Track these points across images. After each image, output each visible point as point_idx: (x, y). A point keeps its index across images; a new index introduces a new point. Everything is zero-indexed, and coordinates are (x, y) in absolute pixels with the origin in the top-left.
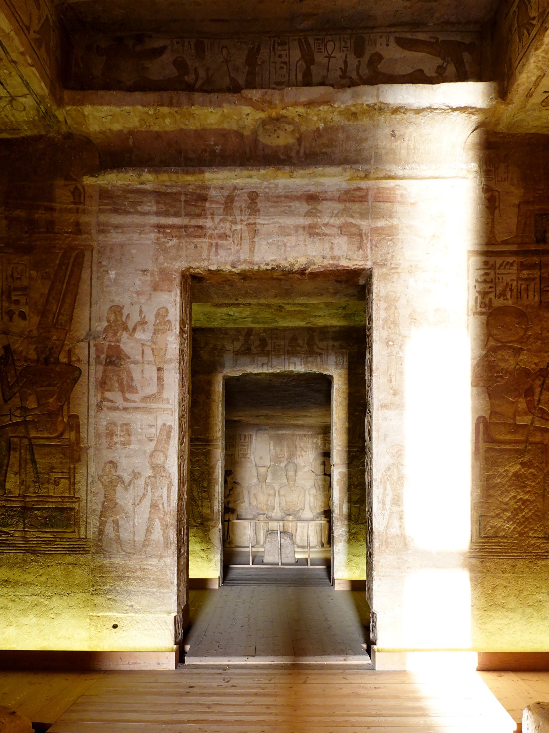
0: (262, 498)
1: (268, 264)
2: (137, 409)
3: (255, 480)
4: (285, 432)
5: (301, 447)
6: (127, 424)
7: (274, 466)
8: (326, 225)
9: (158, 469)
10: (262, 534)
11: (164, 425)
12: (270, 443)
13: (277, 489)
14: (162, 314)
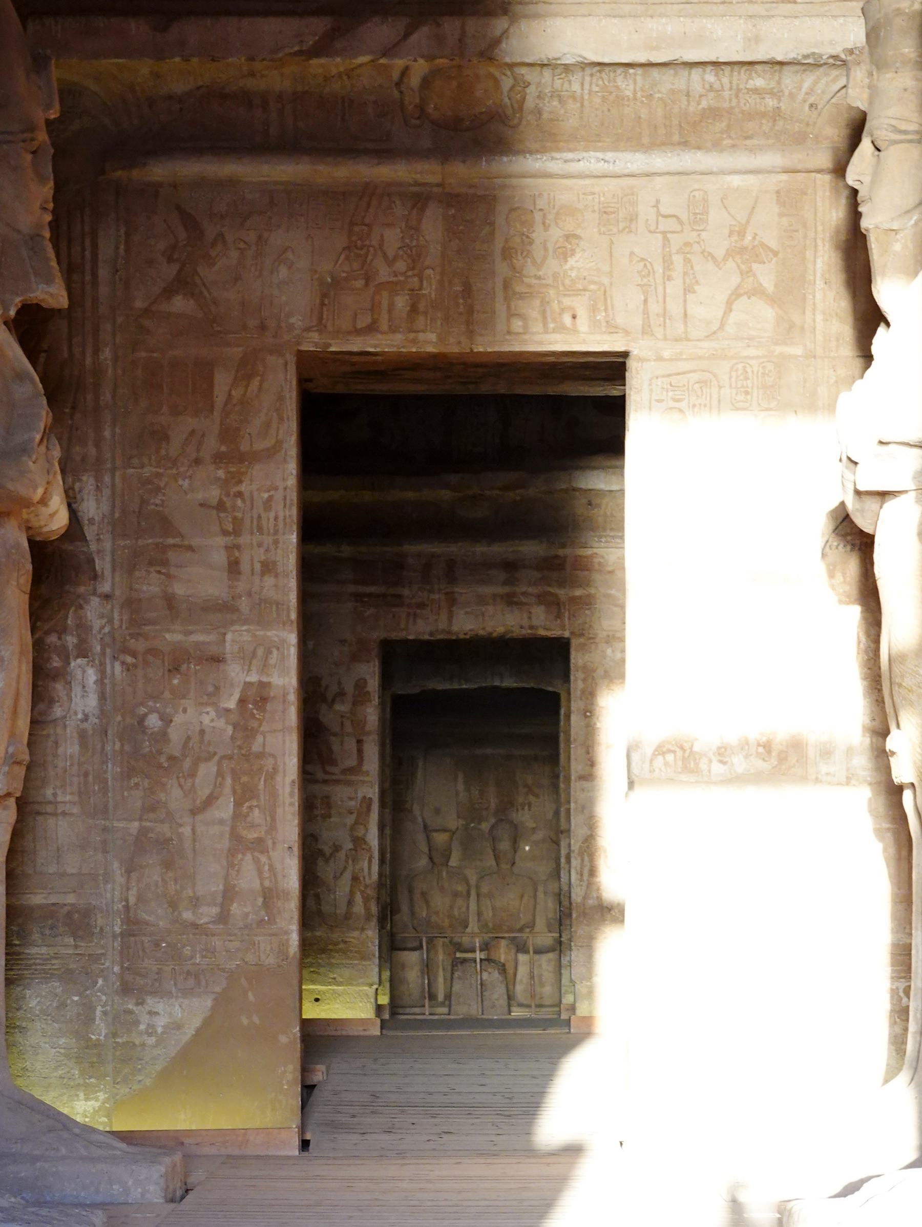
0: (439, 901)
1: (465, 634)
2: (337, 782)
3: (423, 862)
4: (489, 751)
5: (526, 786)
6: (327, 797)
7: (466, 827)
8: (523, 594)
9: (359, 842)
10: (441, 980)
11: (365, 797)
12: (456, 780)
13: (473, 882)
14: (361, 685)
